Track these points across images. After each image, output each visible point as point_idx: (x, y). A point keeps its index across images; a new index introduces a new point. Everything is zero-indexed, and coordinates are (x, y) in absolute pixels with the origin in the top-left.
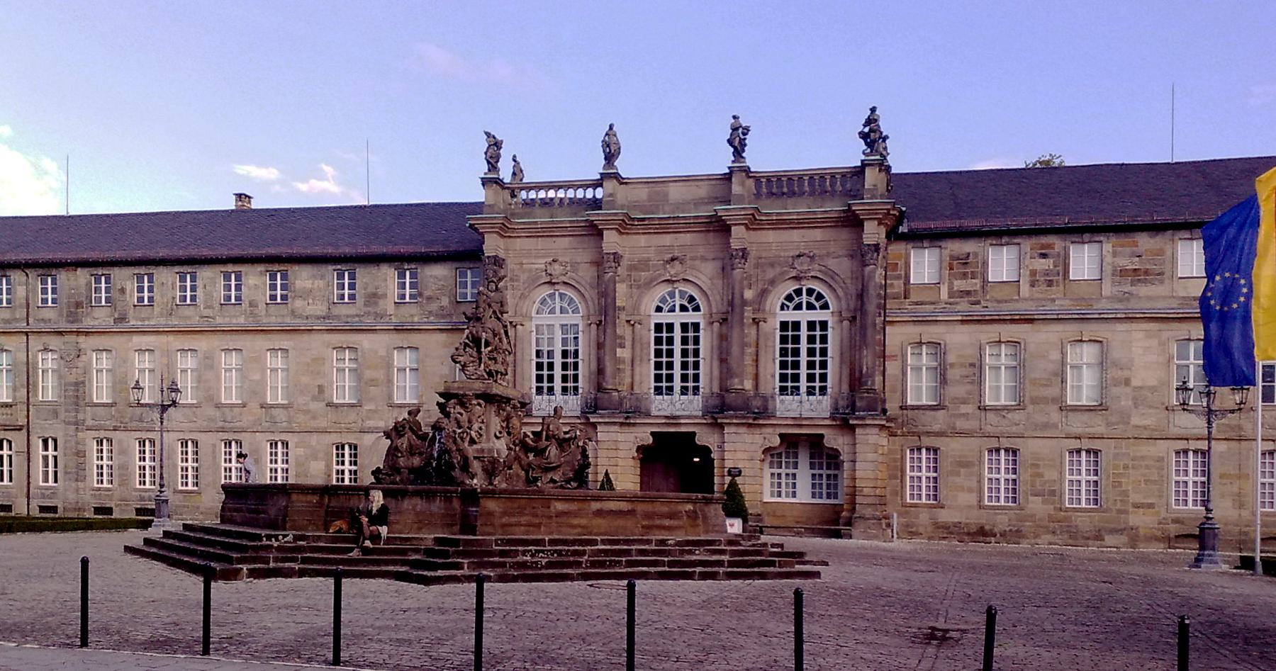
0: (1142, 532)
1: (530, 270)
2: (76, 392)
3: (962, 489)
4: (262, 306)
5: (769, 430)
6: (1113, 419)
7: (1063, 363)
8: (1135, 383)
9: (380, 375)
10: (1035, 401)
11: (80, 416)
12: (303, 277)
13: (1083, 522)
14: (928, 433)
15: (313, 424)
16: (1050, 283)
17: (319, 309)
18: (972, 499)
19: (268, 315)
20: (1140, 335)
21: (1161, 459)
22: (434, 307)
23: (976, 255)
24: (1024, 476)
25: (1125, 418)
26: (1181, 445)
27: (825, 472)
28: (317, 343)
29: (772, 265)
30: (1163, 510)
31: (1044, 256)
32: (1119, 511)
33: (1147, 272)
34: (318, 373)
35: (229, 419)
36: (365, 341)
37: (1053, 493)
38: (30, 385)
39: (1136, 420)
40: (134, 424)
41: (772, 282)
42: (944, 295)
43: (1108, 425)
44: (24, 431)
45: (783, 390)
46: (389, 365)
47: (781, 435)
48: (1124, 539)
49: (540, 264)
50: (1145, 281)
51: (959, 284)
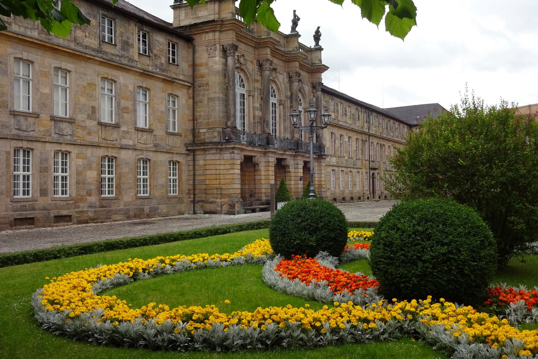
15: (89, 139)
17: (94, 43)
28: (92, 72)
34: (92, 96)
35: (24, 127)
36: (123, 78)
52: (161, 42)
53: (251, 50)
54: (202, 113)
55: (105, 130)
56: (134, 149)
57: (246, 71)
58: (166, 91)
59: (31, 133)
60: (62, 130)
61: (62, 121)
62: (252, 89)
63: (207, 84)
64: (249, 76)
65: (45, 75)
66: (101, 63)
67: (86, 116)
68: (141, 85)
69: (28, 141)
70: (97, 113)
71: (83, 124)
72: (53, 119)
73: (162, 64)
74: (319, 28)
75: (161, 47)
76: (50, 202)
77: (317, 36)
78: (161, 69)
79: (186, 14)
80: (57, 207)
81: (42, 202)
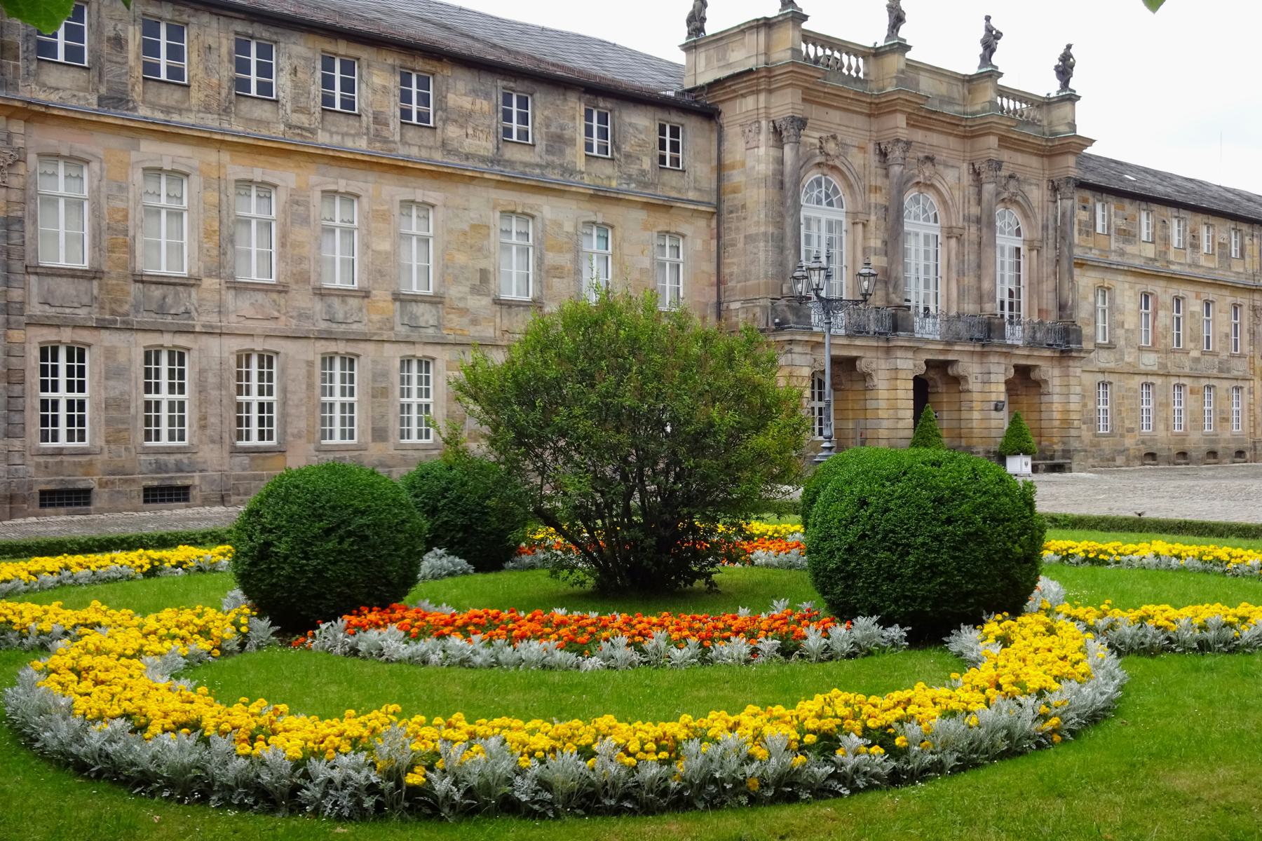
9: (565, 260)
11: (16, 294)
12: (461, 93)
15: (473, 332)
17: (485, 145)
19: (403, 141)
22: (633, 170)
28: (480, 204)
34: (480, 249)
35: (340, 317)
36: (548, 208)
46: (577, 251)
52: (640, 128)
53: (860, 121)
54: (735, 269)
55: (509, 314)
57: (844, 169)
58: (654, 226)
59: (355, 326)
60: (417, 318)
61: (416, 301)
62: (860, 208)
63: (744, 206)
64: (852, 179)
65: (384, 217)
66: (500, 184)
67: (467, 289)
68: (593, 219)
69: (348, 340)
70: (492, 280)
71: (461, 305)
72: (397, 297)
73: (643, 173)
74: (1069, 47)
75: (643, 136)
76: (392, 452)
77: (1065, 69)
78: (639, 183)
79: (708, 60)
81: (375, 452)
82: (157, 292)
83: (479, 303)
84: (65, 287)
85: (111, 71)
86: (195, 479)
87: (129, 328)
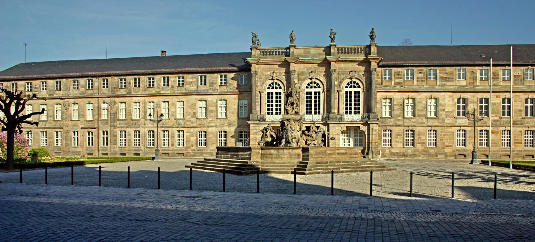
0: (448, 154)
1: (266, 75)
2: (114, 116)
3: (398, 142)
4: (176, 87)
5: (343, 125)
6: (440, 121)
7: (426, 104)
8: (446, 110)
10: (419, 116)
11: (115, 124)
13: (432, 151)
14: (389, 126)
15: (192, 125)
16: (422, 81)
17: (194, 88)
18: (401, 145)
20: (447, 96)
21: (453, 133)
23: (402, 72)
24: (416, 138)
25: (444, 120)
26: (459, 128)
27: (358, 138)
29: (343, 74)
30: (454, 147)
31: (420, 73)
32: (442, 148)
33: (449, 78)
37: (424, 143)
38: (99, 114)
39: (446, 121)
40: (134, 126)
41: (343, 79)
42: (393, 84)
43: (439, 123)
44: (97, 129)
45: (347, 113)
47: (347, 127)
48: (443, 156)
49: (269, 73)
50: (449, 81)
51: (397, 81)
56: (216, 127)
80: (177, 150)
81: (171, 148)
82: (134, 122)
83: (194, 119)
84: (122, 122)
85: (129, 88)
86: (141, 152)
87: (130, 128)
